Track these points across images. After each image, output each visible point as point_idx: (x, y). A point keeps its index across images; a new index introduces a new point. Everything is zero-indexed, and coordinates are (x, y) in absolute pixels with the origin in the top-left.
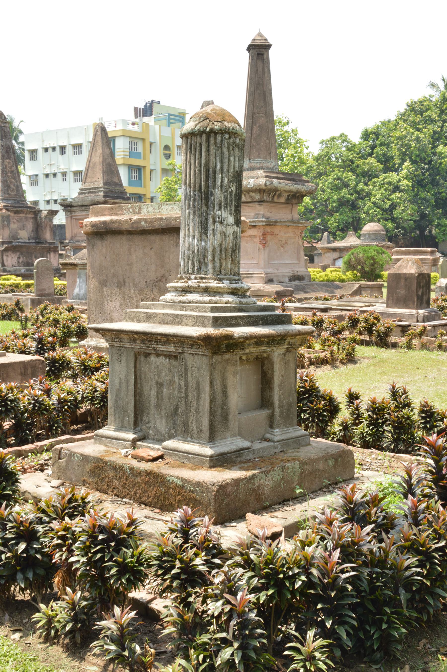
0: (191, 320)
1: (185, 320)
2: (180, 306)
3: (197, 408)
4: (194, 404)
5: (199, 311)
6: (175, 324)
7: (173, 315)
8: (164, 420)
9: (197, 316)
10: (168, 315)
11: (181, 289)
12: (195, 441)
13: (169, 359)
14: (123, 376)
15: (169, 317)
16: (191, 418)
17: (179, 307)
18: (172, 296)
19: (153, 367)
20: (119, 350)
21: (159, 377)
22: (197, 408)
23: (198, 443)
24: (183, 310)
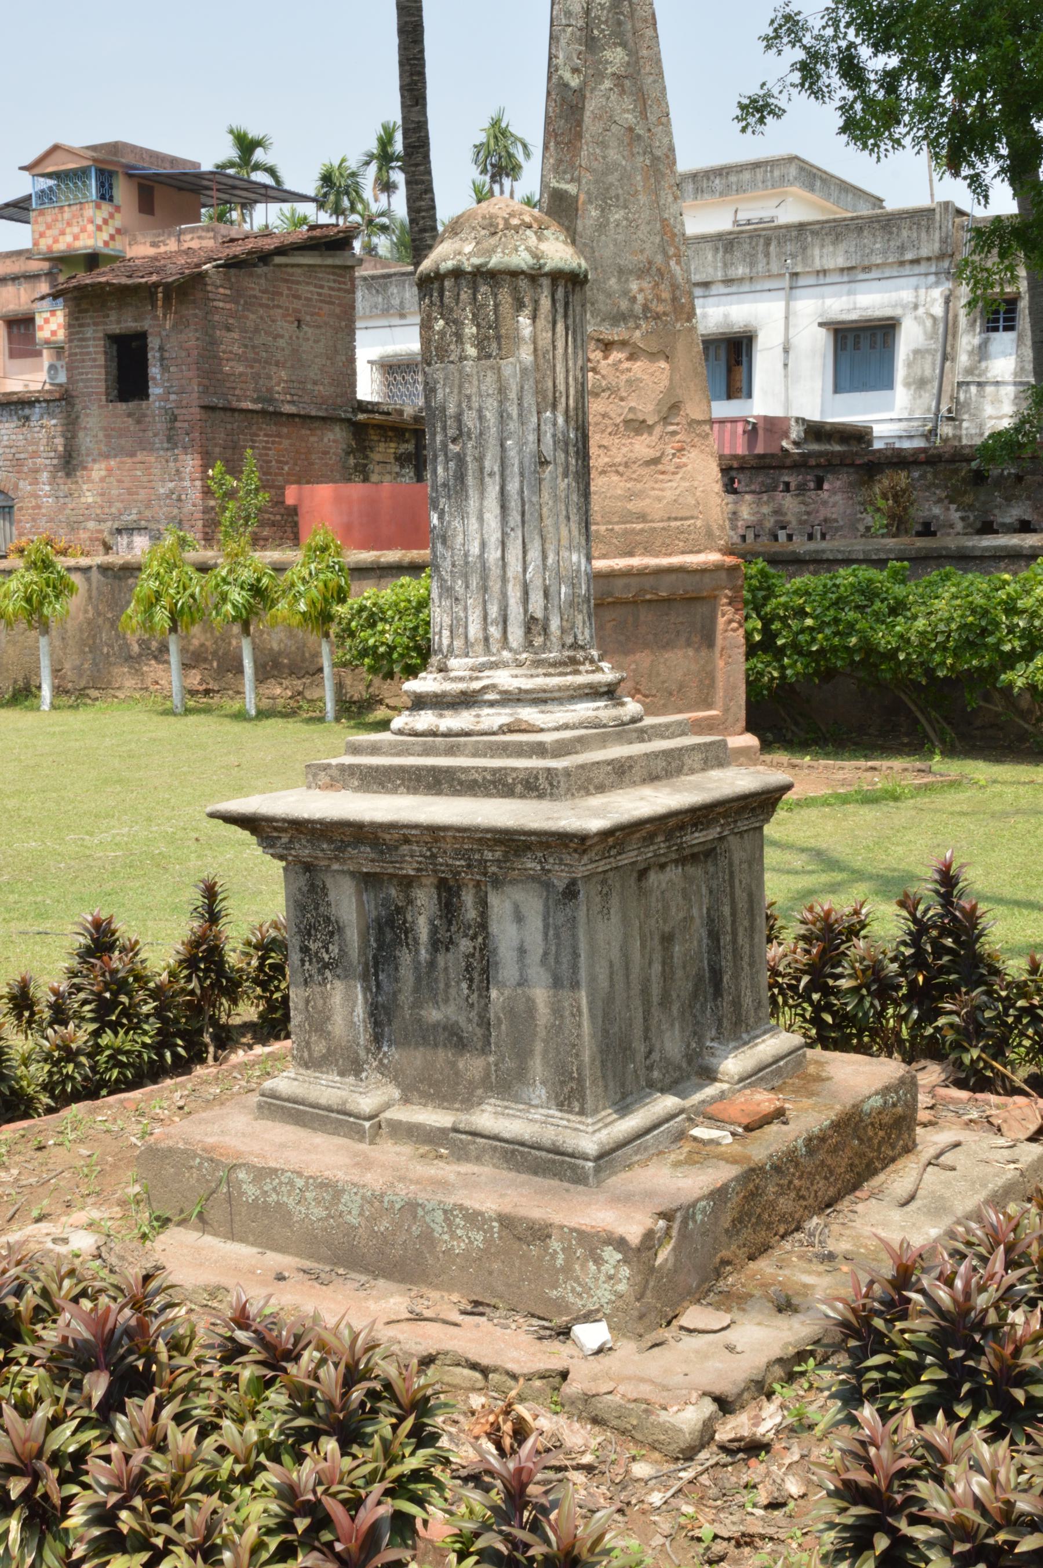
0: (698, 756)
1: (687, 761)
2: (636, 730)
3: (752, 956)
4: (747, 949)
5: (673, 736)
6: (672, 776)
7: (667, 754)
8: (677, 1026)
9: (705, 744)
10: (656, 755)
11: (605, 689)
12: (758, 1032)
13: (683, 865)
14: (615, 954)
15: (659, 761)
16: (743, 984)
17: (635, 735)
18: (598, 708)
19: (654, 899)
20: (604, 882)
21: (665, 921)
22: (752, 956)
23: (765, 1033)
24: (643, 741)
